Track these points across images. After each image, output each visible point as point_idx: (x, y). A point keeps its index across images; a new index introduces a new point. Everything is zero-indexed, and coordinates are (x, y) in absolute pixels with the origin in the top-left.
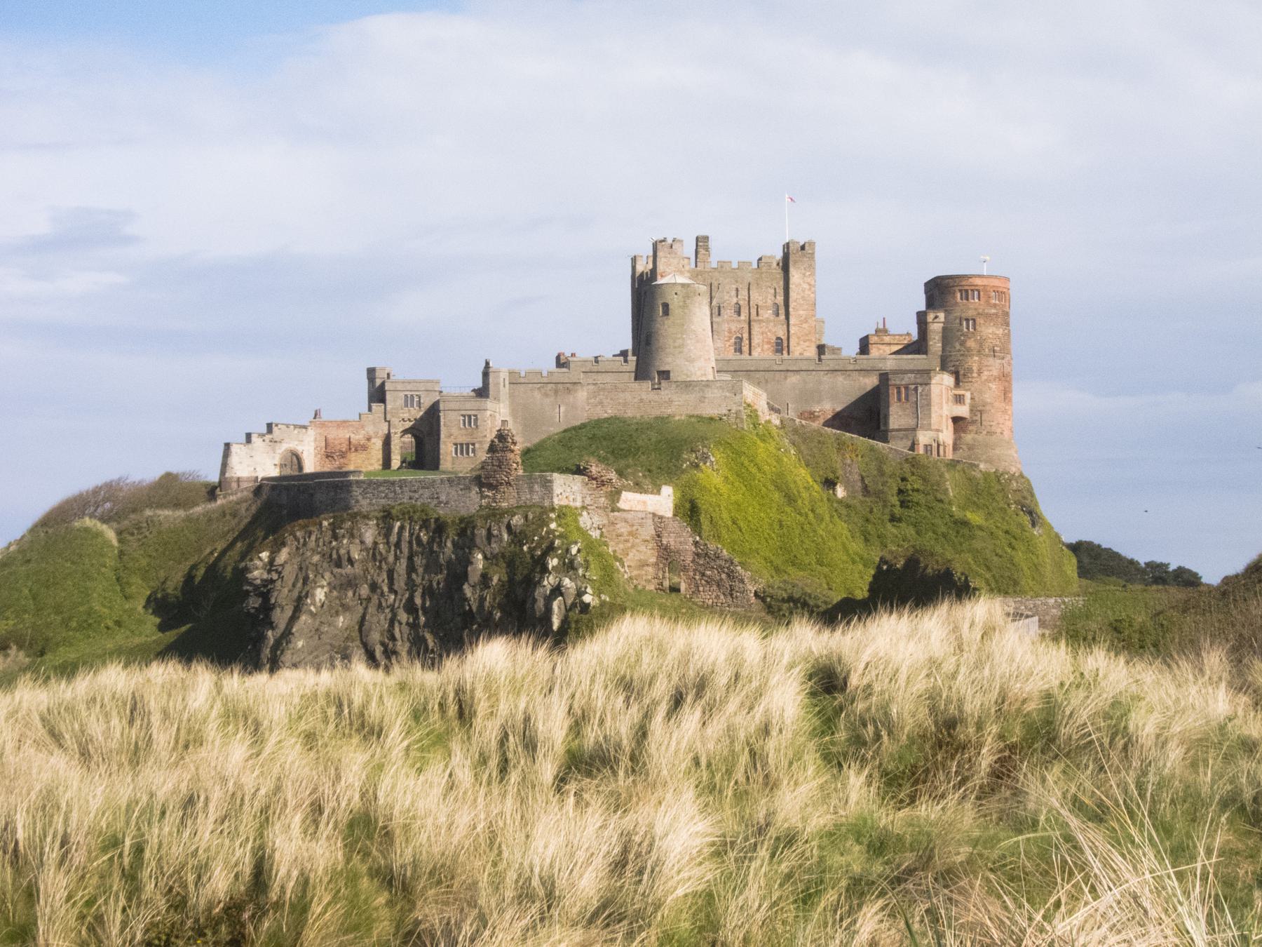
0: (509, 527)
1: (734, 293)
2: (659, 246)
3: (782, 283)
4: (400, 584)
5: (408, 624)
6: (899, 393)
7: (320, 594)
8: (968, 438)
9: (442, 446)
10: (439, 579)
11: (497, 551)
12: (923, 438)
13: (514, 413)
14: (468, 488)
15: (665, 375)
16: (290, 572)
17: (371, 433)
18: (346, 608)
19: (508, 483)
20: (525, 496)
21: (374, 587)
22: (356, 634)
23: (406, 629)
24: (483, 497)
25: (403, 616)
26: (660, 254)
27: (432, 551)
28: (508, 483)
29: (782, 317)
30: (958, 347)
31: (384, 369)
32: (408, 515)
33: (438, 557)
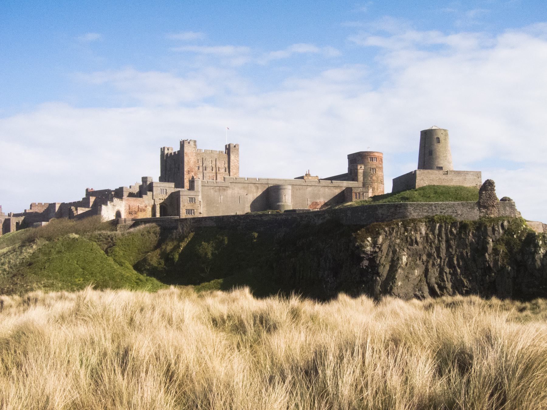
0: (502, 225)
1: (210, 162)
2: (185, 142)
3: (227, 159)
4: (443, 254)
5: (450, 273)
6: (356, 195)
7: (404, 259)
9: (181, 210)
10: (467, 252)
11: (498, 238)
13: (203, 197)
14: (473, 208)
15: (441, 168)
16: (385, 248)
17: (147, 204)
18: (417, 266)
19: (493, 206)
20: (502, 212)
21: (429, 255)
22: (424, 279)
23: (449, 276)
24: (481, 212)
25: (447, 270)
26: (185, 145)
27: (460, 238)
28: (493, 206)
29: (227, 172)
30: (370, 179)
31: (150, 177)
32: (443, 220)
33: (465, 241)
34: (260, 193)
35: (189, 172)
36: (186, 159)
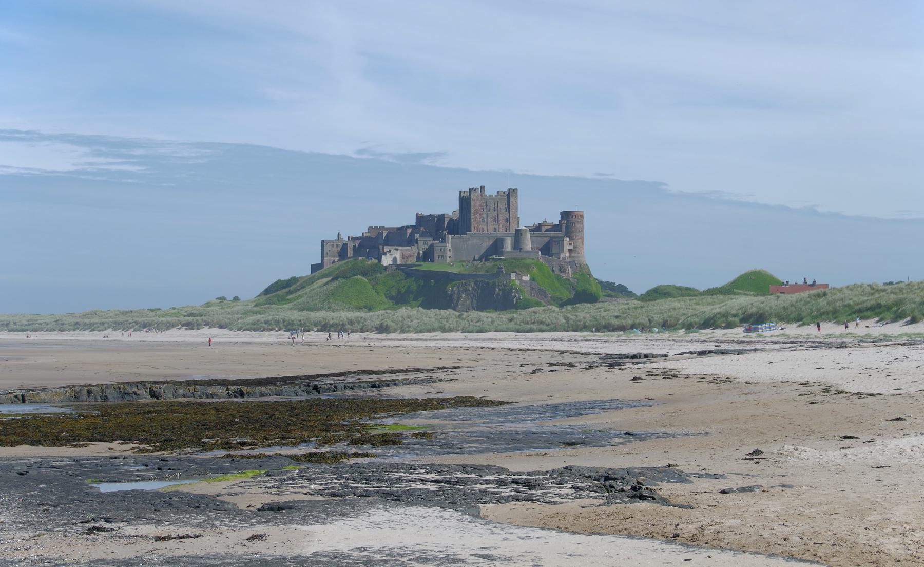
8: (573, 255)
12: (562, 255)
15: (521, 249)
36: (472, 203)
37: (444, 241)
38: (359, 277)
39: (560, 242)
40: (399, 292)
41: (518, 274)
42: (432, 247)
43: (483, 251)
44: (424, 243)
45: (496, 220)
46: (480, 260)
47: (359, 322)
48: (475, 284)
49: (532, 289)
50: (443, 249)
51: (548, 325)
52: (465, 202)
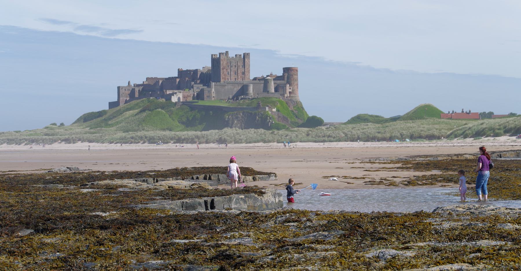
8: (292, 95)
12: (286, 95)
15: (268, 92)
34: (240, 88)
35: (223, 69)
36: (221, 62)
37: (209, 86)
38: (160, 110)
39: (284, 88)
40: (188, 119)
41: (269, 108)
42: (202, 91)
43: (235, 93)
44: (198, 87)
45: (236, 73)
46: (233, 98)
47: (203, 137)
48: (243, 114)
49: (279, 117)
50: (210, 92)
51: (334, 138)
52: (216, 61)
